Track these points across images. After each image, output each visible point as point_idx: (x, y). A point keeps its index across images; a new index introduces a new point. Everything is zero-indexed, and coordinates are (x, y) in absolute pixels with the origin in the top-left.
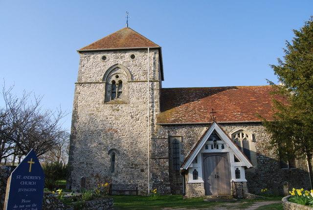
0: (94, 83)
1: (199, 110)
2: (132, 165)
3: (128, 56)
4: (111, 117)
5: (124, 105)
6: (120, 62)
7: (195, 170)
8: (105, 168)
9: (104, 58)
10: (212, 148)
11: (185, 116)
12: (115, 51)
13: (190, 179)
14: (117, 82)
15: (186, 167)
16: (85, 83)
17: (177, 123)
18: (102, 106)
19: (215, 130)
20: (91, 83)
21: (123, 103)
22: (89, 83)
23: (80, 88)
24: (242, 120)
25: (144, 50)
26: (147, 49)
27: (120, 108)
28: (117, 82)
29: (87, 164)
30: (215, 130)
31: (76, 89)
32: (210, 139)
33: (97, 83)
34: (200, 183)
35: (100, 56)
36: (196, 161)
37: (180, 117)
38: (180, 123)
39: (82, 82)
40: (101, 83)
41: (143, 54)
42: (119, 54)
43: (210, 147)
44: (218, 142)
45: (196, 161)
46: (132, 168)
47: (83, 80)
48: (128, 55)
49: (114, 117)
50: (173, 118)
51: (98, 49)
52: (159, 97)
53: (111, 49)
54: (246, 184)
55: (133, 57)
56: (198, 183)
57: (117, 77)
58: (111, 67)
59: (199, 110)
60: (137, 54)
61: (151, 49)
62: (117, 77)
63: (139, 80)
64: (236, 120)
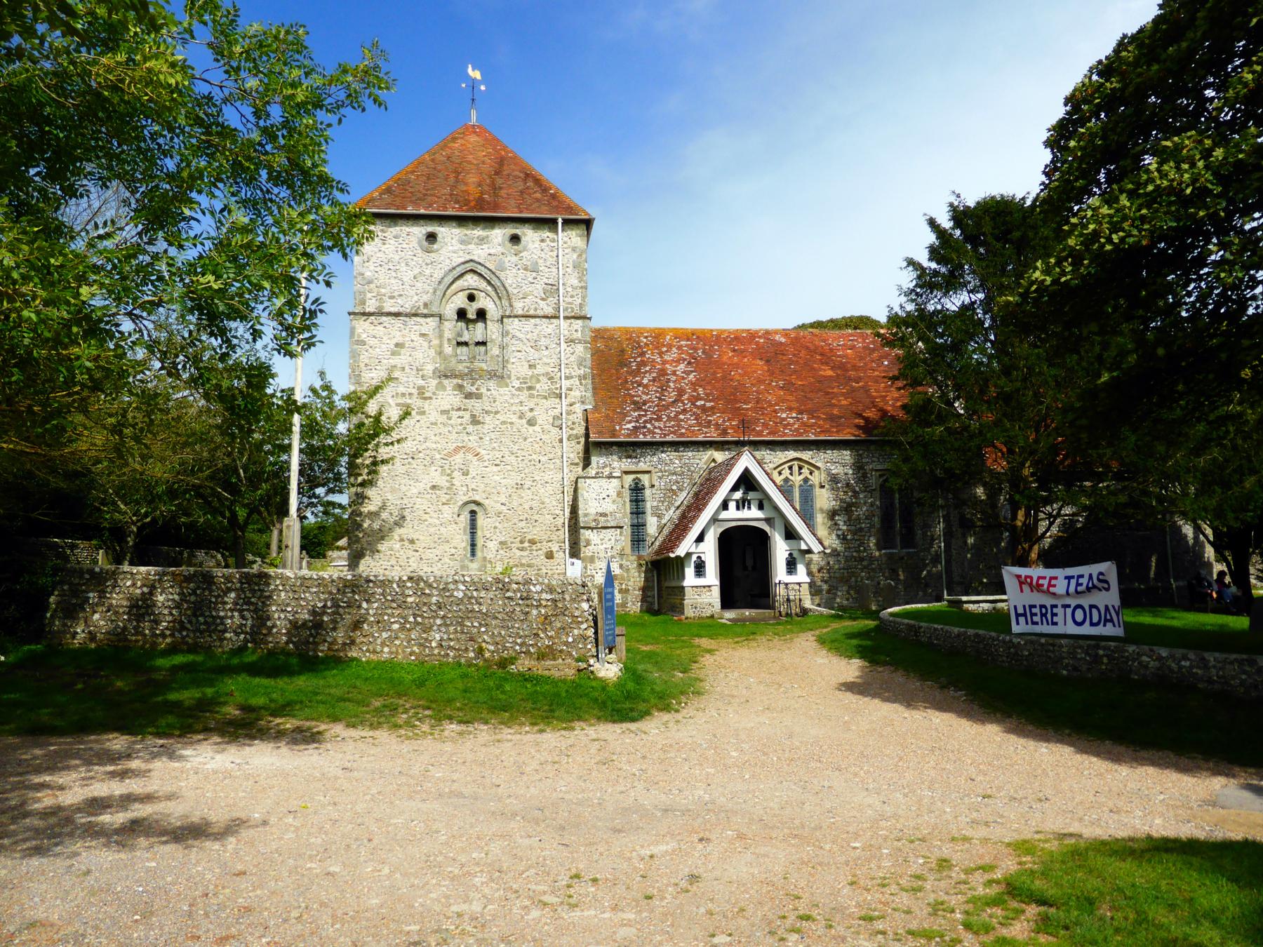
0: (406, 315)
1: (693, 400)
2: (522, 542)
3: (500, 239)
4: (461, 413)
5: (492, 384)
6: (479, 253)
7: (699, 557)
8: (453, 551)
9: (432, 237)
10: (738, 508)
11: (659, 419)
12: (461, 221)
13: (690, 578)
14: (471, 315)
15: (681, 551)
16: (380, 313)
17: (641, 438)
18: (434, 382)
19: (747, 471)
20: (397, 315)
21: (493, 375)
22: (389, 314)
23: (362, 326)
24: (801, 434)
25: (550, 223)
26: (554, 221)
27: (483, 390)
28: (471, 315)
29: (402, 540)
30: (747, 471)
31: (352, 330)
32: (735, 488)
33: (416, 315)
34: (709, 586)
35: (419, 231)
36: (700, 539)
37: (646, 422)
38: (648, 439)
39: (372, 310)
40: (425, 316)
41: (546, 234)
42: (478, 232)
43: (732, 505)
44: (751, 495)
45: (700, 539)
46: (522, 549)
47: (371, 306)
48: (499, 234)
49: (467, 416)
50: (630, 422)
51: (410, 210)
52: (589, 363)
53: (450, 212)
54: (807, 585)
55: (515, 239)
56: (704, 587)
57: (471, 298)
58: (454, 268)
59: (693, 400)
60: (530, 236)
61: (567, 222)
62: (471, 298)
63: (532, 312)
64: (785, 434)
